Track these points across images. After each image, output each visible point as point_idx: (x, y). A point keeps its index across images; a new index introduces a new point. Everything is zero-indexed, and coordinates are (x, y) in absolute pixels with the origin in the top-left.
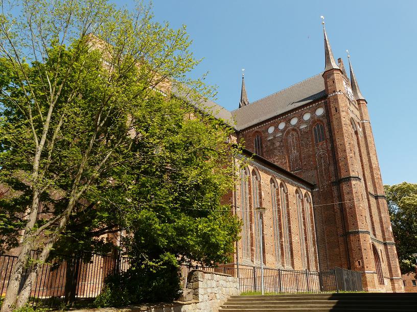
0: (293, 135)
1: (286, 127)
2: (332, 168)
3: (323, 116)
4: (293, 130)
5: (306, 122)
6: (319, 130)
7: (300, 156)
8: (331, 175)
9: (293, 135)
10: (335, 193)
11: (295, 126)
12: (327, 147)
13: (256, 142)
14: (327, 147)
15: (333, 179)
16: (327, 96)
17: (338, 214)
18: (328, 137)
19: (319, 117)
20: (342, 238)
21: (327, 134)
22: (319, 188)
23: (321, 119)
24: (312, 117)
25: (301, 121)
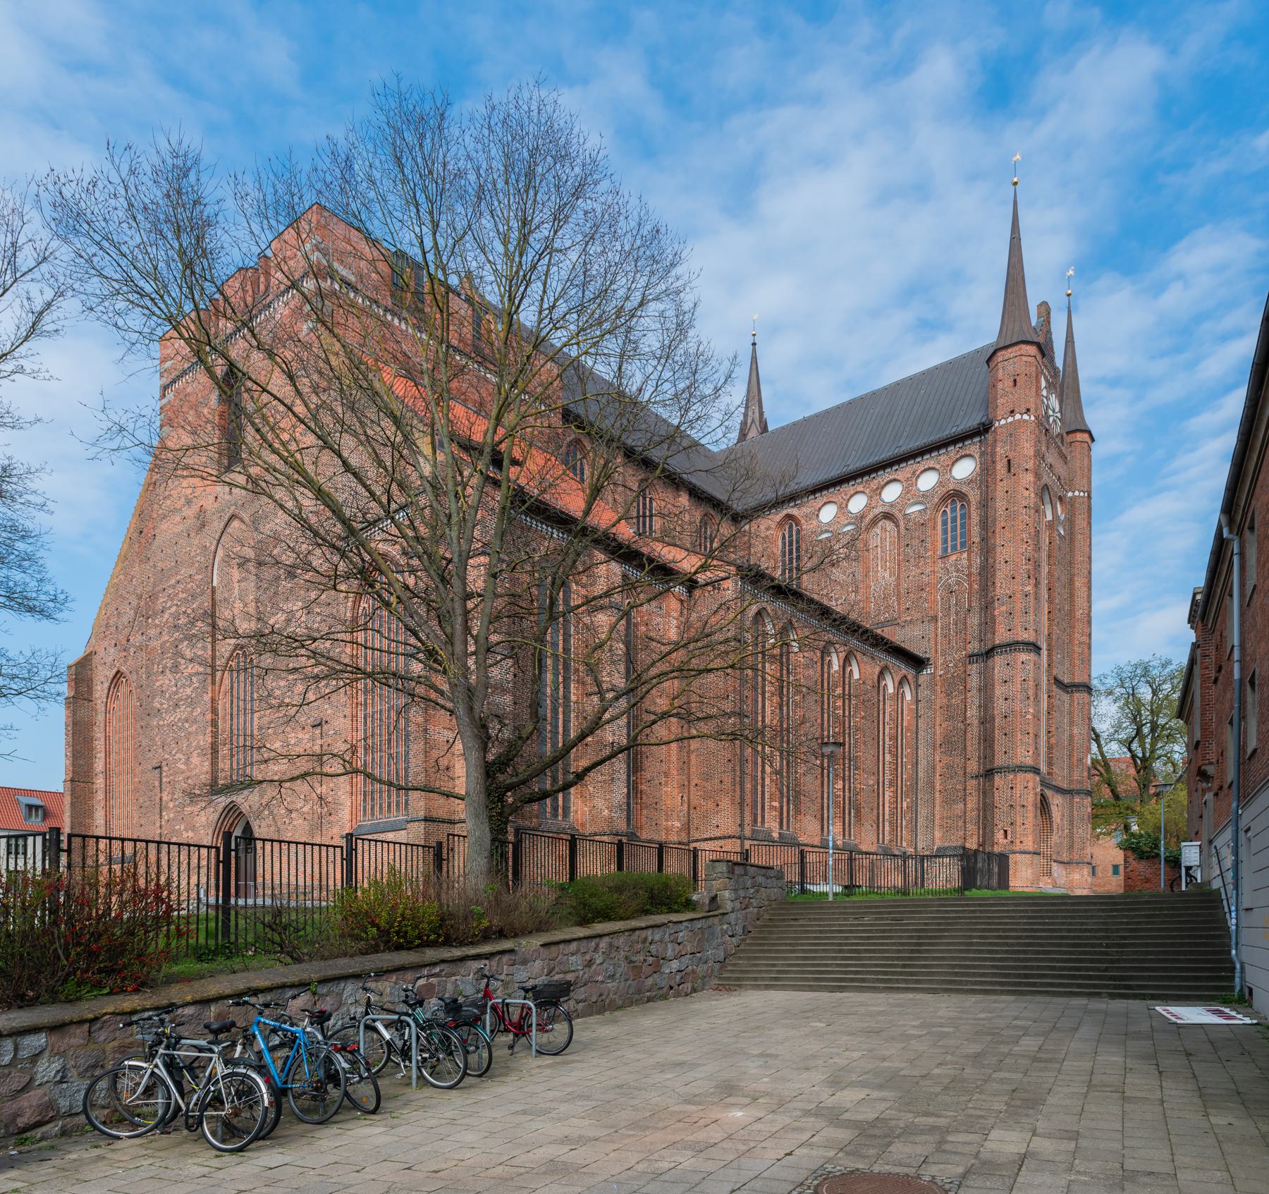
0: (884, 529)
1: (869, 507)
2: (974, 620)
3: (969, 481)
4: (888, 516)
5: (925, 495)
6: (954, 520)
7: (898, 585)
8: (969, 638)
9: (884, 529)
10: (974, 682)
11: (892, 505)
12: (970, 566)
13: (784, 544)
14: (970, 566)
15: (974, 647)
16: (991, 424)
17: (974, 731)
18: (977, 540)
19: (960, 482)
20: (974, 782)
21: (975, 531)
22: (936, 668)
23: (964, 489)
24: (940, 484)
25: (910, 491)
